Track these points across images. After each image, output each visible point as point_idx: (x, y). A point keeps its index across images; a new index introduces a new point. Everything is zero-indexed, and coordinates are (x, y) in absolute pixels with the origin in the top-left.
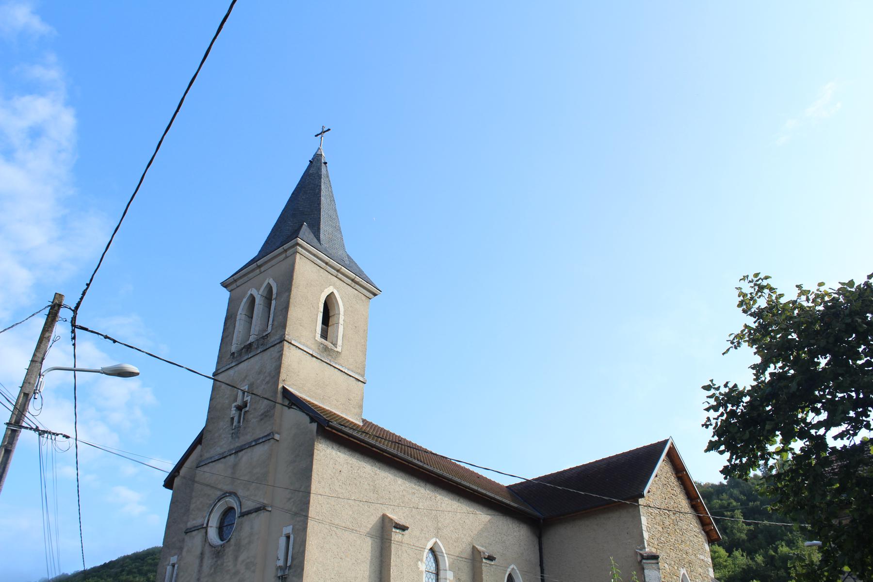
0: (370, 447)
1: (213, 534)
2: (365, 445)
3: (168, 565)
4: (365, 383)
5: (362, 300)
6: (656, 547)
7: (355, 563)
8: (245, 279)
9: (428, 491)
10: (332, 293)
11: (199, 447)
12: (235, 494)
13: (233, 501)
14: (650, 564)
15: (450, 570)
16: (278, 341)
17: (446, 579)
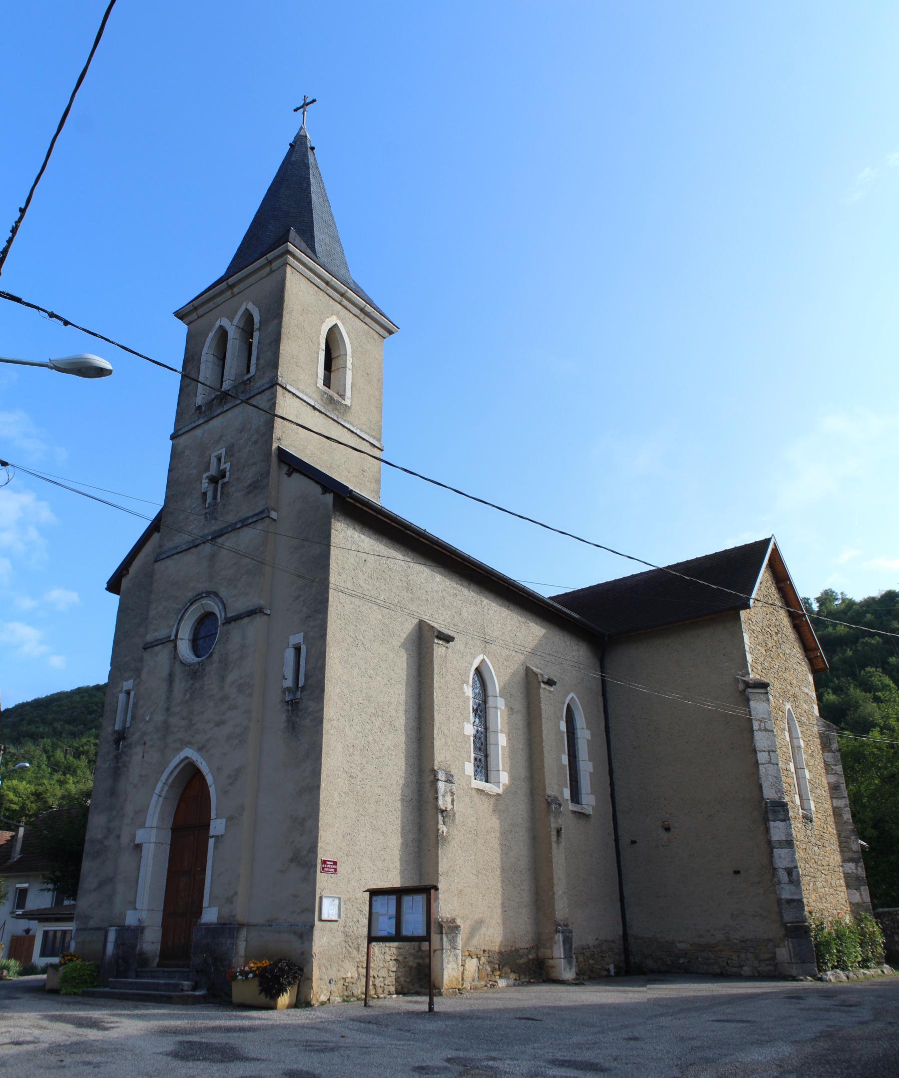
0: (403, 529)
1: (184, 648)
2: (397, 526)
3: (121, 692)
4: (382, 450)
5: (374, 339)
6: (760, 673)
7: (388, 683)
8: (211, 305)
9: (472, 593)
10: (336, 325)
11: (156, 537)
12: (216, 594)
13: (213, 604)
14: (757, 695)
15: (500, 697)
16: (267, 386)
17: (496, 708)
